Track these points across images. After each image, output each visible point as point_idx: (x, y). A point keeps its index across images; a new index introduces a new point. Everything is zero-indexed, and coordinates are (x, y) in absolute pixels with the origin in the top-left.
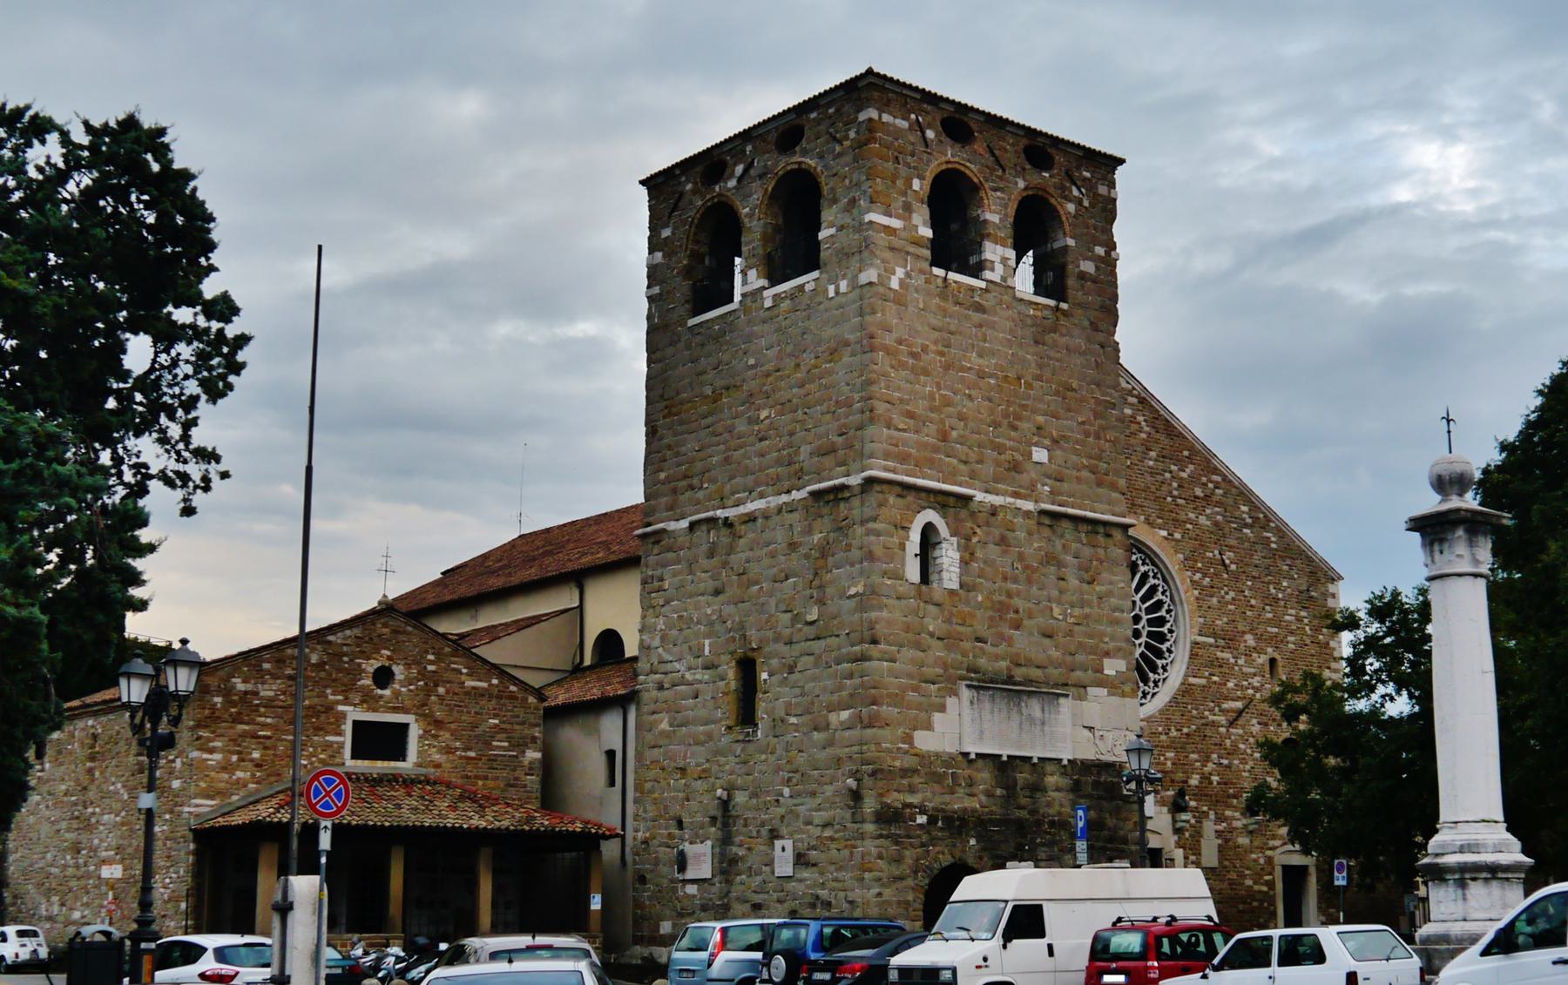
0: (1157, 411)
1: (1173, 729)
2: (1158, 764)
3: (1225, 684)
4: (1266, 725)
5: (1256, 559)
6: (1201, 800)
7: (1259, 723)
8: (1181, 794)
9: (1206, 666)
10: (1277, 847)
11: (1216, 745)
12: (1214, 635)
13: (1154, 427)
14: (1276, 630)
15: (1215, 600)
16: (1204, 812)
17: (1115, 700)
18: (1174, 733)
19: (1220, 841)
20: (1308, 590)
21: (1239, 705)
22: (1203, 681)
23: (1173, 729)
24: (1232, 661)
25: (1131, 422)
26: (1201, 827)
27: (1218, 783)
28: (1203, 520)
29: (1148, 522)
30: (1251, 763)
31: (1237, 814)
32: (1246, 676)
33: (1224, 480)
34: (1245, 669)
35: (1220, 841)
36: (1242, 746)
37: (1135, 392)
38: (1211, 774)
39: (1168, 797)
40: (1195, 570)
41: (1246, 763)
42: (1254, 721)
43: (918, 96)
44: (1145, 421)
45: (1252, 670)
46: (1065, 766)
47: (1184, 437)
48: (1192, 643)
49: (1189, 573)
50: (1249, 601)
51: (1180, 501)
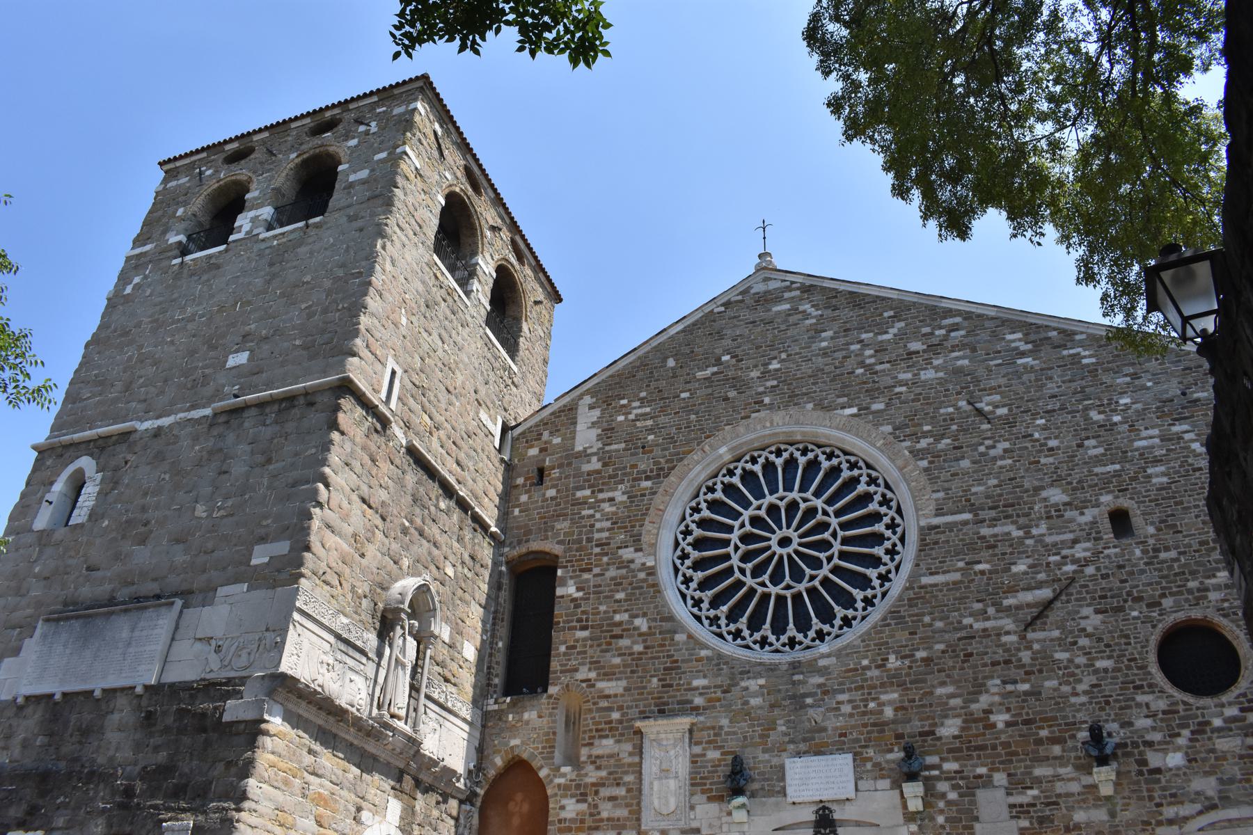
0: (834, 289)
1: (892, 658)
2: (864, 713)
3: (1009, 569)
4: (1120, 609)
5: (1051, 388)
6: (970, 757)
7: (1097, 612)
8: (909, 752)
9: (957, 554)
10: (1186, 819)
11: (994, 664)
12: (973, 508)
13: (825, 308)
14: (1118, 467)
15: (965, 464)
16: (980, 776)
17: (259, 594)
18: (893, 662)
19: (1025, 823)
20: (1184, 394)
21: (1046, 593)
22: (957, 576)
23: (892, 658)
24: (1017, 533)
25: (790, 315)
26: (973, 803)
27: (1008, 724)
28: (928, 375)
29: (821, 406)
30: (1093, 680)
31: (1066, 771)
32: (1055, 548)
33: (965, 319)
34: (1048, 540)
35: (1025, 823)
36: (1062, 656)
37: (794, 286)
38: (988, 712)
39: (893, 761)
40: (916, 437)
41: (1080, 681)
42: (1091, 609)
43: (204, 155)
44: (813, 306)
45: (1070, 536)
46: (140, 696)
47: (884, 299)
48: (921, 529)
49: (908, 444)
50: (1046, 445)
51: (879, 368)
